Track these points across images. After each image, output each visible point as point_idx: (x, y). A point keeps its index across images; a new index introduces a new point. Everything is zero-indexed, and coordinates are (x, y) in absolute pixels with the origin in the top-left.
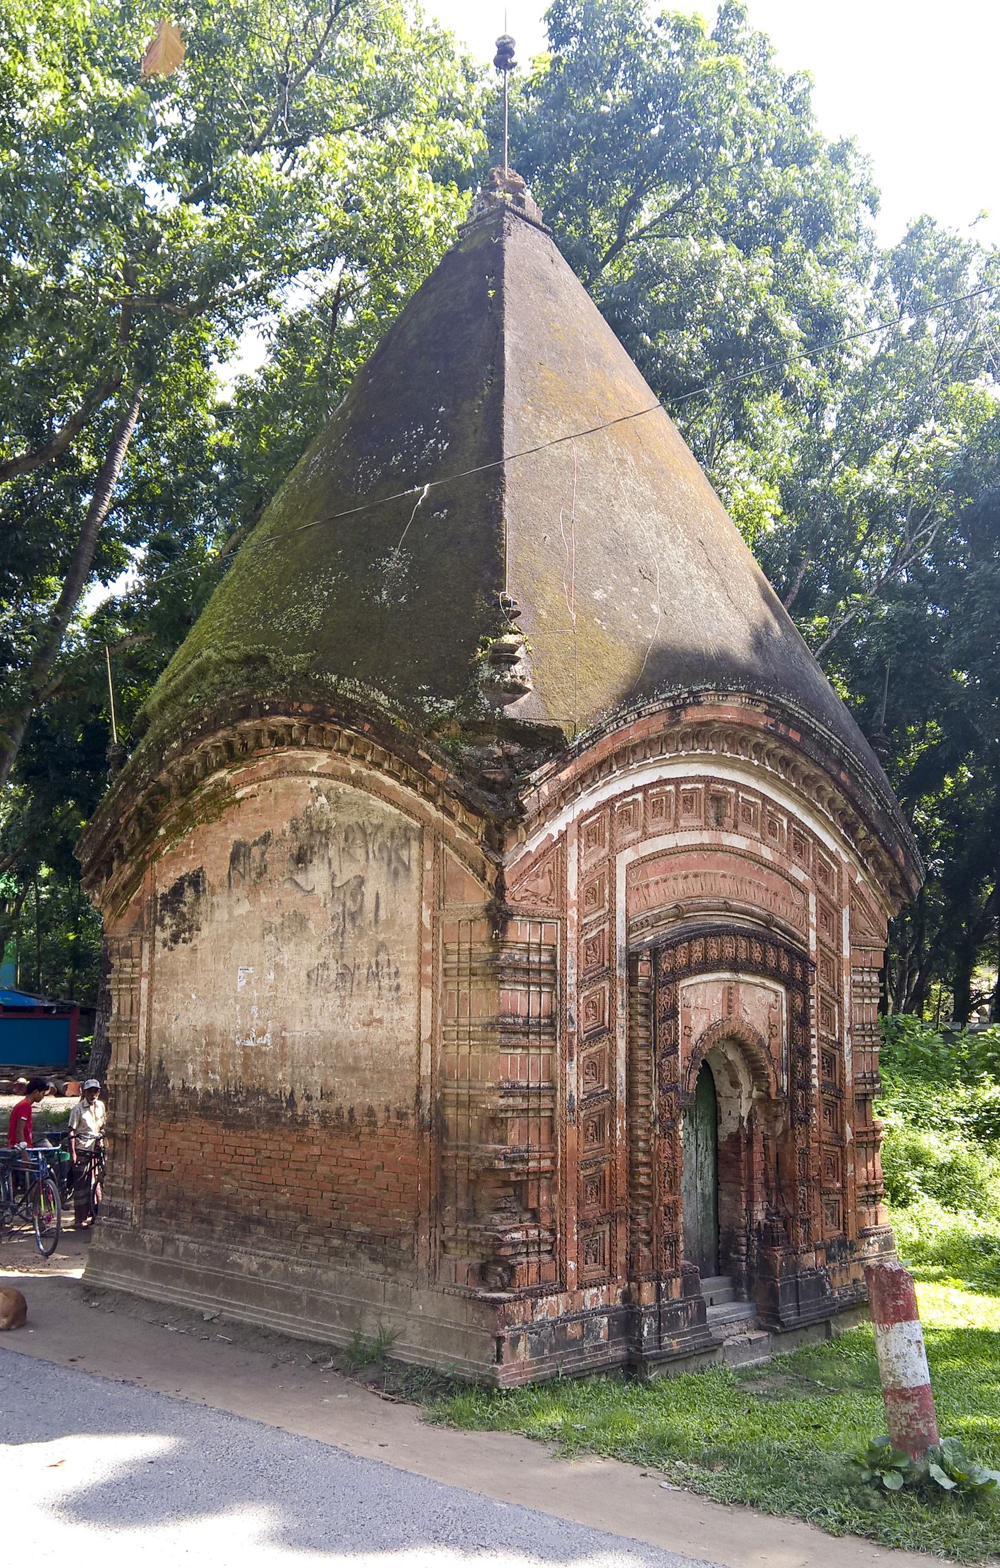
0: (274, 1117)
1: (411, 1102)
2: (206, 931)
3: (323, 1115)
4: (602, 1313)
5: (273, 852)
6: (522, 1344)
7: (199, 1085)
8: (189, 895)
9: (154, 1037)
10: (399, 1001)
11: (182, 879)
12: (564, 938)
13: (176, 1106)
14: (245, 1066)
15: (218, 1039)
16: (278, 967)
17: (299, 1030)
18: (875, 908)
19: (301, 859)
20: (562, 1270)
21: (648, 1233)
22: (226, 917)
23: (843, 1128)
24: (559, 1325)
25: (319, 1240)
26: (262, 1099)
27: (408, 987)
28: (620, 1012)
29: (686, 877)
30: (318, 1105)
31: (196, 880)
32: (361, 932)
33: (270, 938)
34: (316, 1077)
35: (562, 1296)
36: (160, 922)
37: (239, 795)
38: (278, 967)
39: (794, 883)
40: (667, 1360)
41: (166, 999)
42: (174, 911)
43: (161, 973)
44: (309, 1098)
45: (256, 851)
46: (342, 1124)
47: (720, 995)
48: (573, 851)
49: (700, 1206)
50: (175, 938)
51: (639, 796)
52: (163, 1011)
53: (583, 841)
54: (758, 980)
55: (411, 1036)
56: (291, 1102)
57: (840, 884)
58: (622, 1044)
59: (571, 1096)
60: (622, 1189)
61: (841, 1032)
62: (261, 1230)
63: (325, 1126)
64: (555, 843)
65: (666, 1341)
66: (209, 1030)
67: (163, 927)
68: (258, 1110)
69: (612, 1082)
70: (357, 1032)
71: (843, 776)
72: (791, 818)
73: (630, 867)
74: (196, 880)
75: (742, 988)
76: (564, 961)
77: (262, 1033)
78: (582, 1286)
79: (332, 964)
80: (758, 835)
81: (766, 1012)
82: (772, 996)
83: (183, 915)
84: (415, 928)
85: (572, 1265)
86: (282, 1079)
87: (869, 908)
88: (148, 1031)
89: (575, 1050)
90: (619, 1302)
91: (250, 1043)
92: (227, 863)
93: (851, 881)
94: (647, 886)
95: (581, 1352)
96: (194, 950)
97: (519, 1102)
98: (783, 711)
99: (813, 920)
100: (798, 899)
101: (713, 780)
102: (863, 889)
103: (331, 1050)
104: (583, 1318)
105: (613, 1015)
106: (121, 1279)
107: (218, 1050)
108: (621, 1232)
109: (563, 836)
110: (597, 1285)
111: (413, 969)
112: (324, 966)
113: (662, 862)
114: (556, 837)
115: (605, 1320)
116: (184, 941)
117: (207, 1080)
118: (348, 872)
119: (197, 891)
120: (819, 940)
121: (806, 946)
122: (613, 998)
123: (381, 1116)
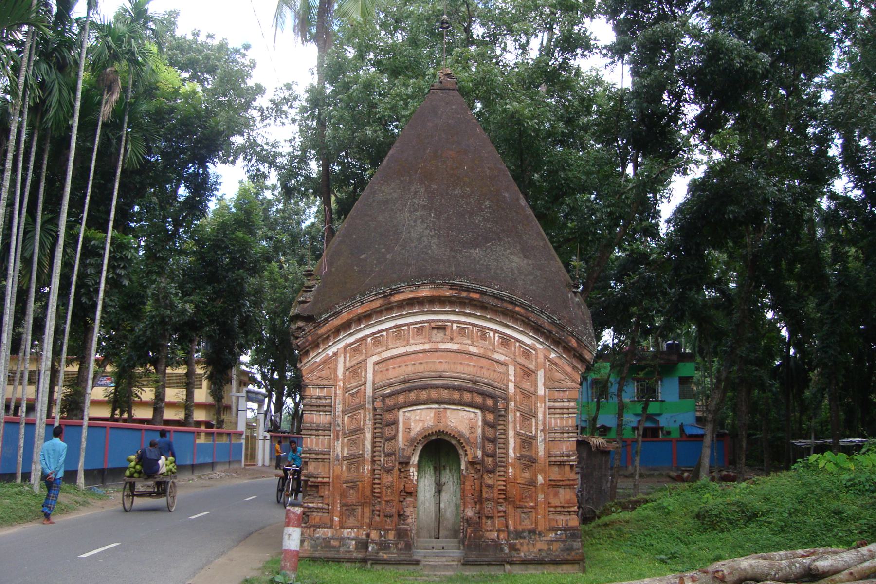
4: (353, 539)
6: (306, 543)
12: (336, 393)
18: (569, 369)
20: (332, 520)
21: (379, 511)
23: (536, 477)
24: (327, 541)
28: (368, 422)
29: (414, 364)
35: (330, 530)
39: (497, 362)
40: (377, 562)
47: (432, 415)
48: (341, 359)
49: (454, 509)
51: (385, 333)
53: (348, 355)
54: (459, 408)
57: (536, 359)
58: (369, 436)
59: (337, 455)
60: (368, 492)
61: (536, 431)
64: (331, 357)
65: (381, 554)
69: (364, 451)
71: (517, 309)
72: (495, 331)
73: (377, 363)
75: (448, 412)
76: (335, 402)
78: (342, 527)
80: (470, 342)
81: (467, 421)
82: (472, 415)
85: (336, 519)
87: (563, 369)
89: (340, 437)
90: (364, 537)
93: (546, 357)
94: (387, 370)
95: (338, 551)
97: (314, 456)
98: (461, 286)
99: (513, 378)
100: (501, 369)
101: (433, 321)
102: (557, 361)
104: (341, 539)
105: (365, 423)
108: (367, 510)
109: (335, 354)
110: (352, 528)
113: (398, 360)
114: (331, 354)
115: (354, 542)
120: (516, 387)
121: (506, 390)
122: (365, 416)
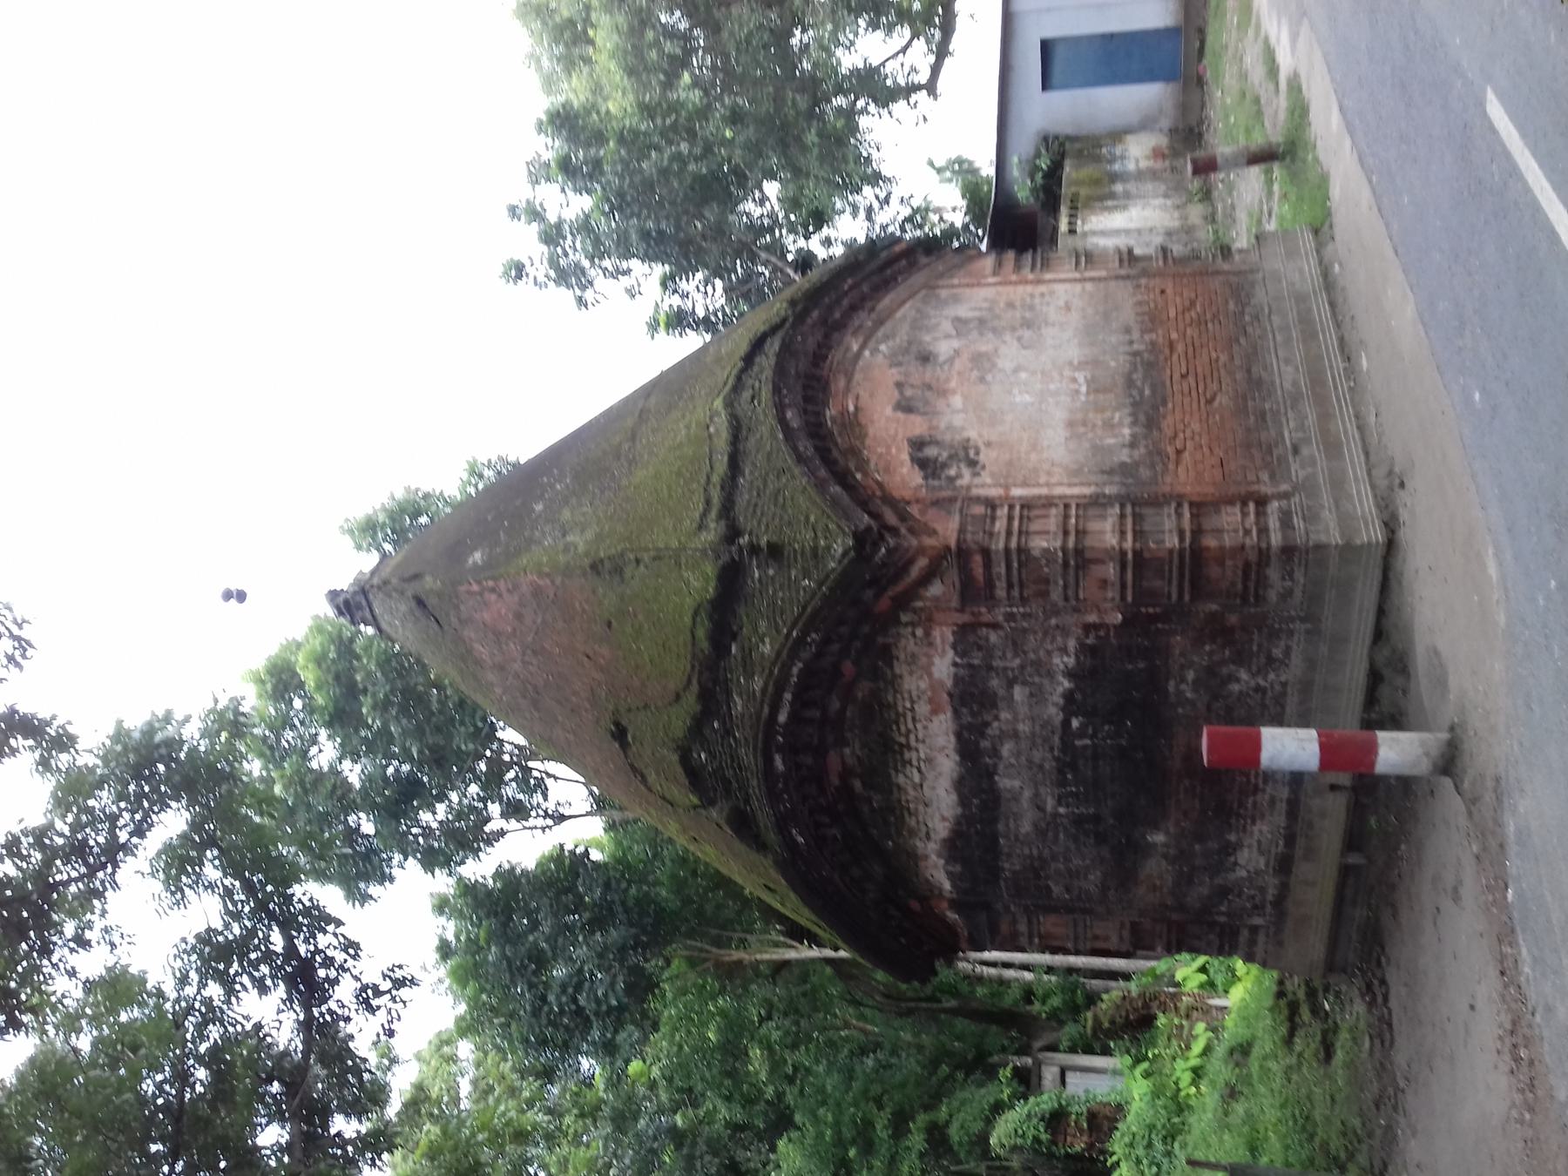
0: (1150, 366)
1: (1128, 283)
2: (972, 434)
3: (1143, 332)
5: (916, 379)
7: (1127, 431)
8: (931, 452)
9: (1076, 480)
10: (1052, 293)
11: (913, 459)
13: (1150, 453)
14: (1105, 390)
15: (1079, 416)
16: (1016, 370)
17: (1074, 352)
19: (926, 358)
22: (962, 415)
25: (1250, 330)
26: (1135, 376)
27: (1043, 288)
30: (1136, 335)
31: (917, 444)
32: (998, 317)
33: (989, 377)
34: (1114, 339)
36: (951, 480)
37: (851, 408)
38: (1016, 370)
41: (1035, 470)
42: (944, 466)
43: (1007, 477)
44: (1131, 342)
45: (909, 392)
46: (1152, 319)
50: (972, 464)
52: (1049, 474)
55: (1078, 287)
56: (1135, 354)
62: (1254, 369)
63: (1151, 331)
66: (1070, 424)
67: (959, 476)
68: (1145, 378)
70: (1075, 316)
74: (917, 444)
77: (1074, 380)
79: (1020, 332)
83: (951, 457)
84: (1000, 288)
86: (1117, 363)
88: (1070, 485)
91: (1084, 389)
92: (912, 417)
96: (988, 444)
103: (1089, 332)
106: (1359, 492)
107: (1091, 415)
111: (1029, 288)
112: (1019, 339)
116: (977, 453)
117: (1121, 424)
118: (947, 326)
119: (930, 443)
123: (1139, 297)
